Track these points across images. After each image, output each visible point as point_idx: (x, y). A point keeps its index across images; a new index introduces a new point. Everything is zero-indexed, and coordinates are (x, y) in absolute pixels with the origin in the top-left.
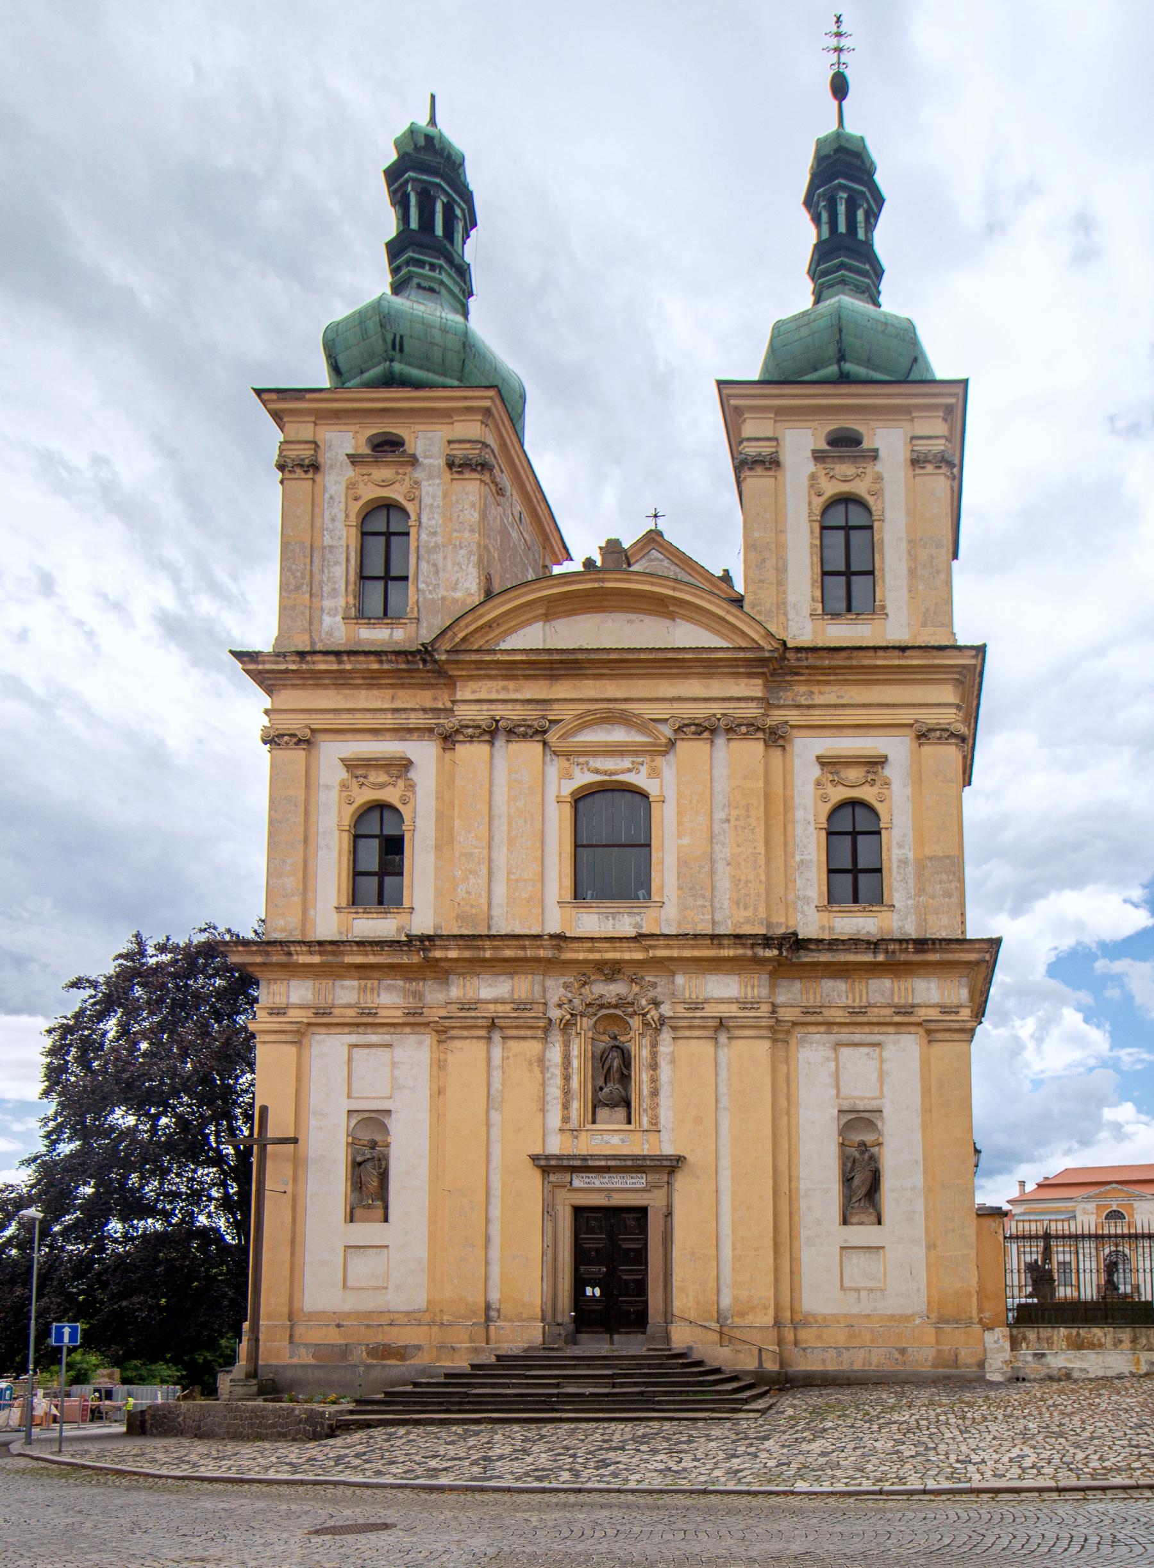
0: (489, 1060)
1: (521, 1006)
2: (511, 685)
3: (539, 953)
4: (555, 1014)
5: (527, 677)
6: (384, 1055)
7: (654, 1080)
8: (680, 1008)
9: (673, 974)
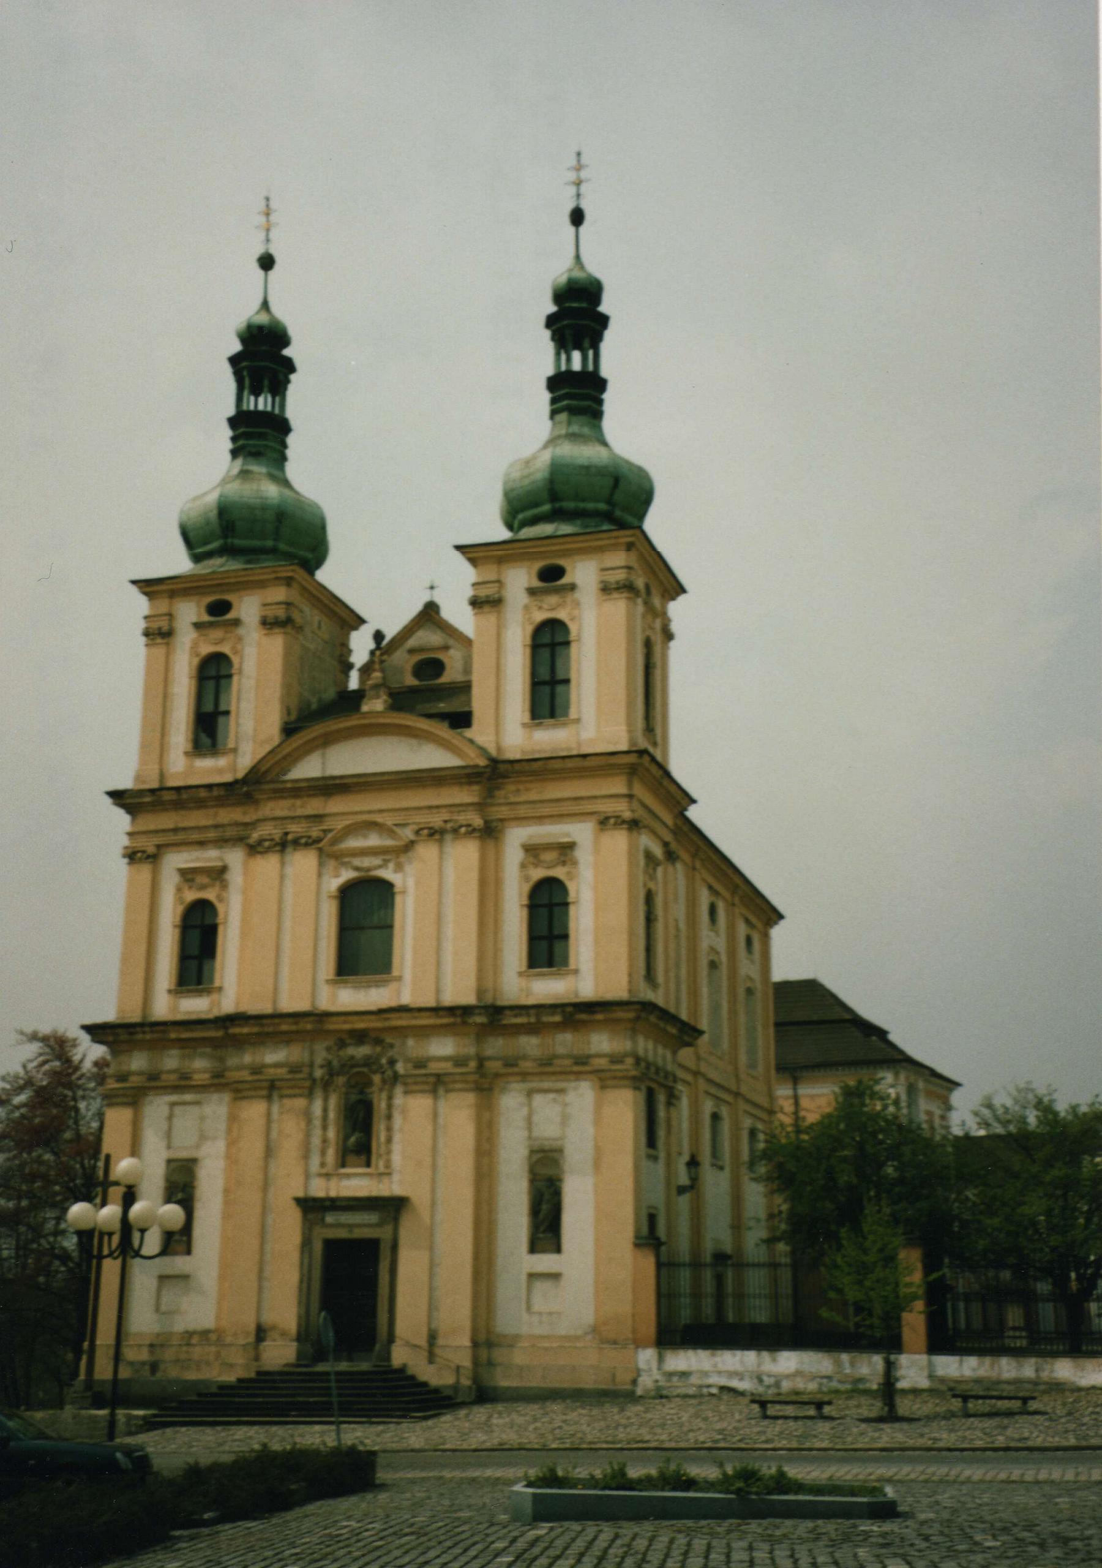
0: (269, 1114)
1: (294, 1069)
2: (298, 802)
3: (310, 1024)
4: (318, 1073)
5: (310, 796)
6: (194, 1110)
7: (389, 1129)
8: (410, 1065)
9: (406, 1037)
